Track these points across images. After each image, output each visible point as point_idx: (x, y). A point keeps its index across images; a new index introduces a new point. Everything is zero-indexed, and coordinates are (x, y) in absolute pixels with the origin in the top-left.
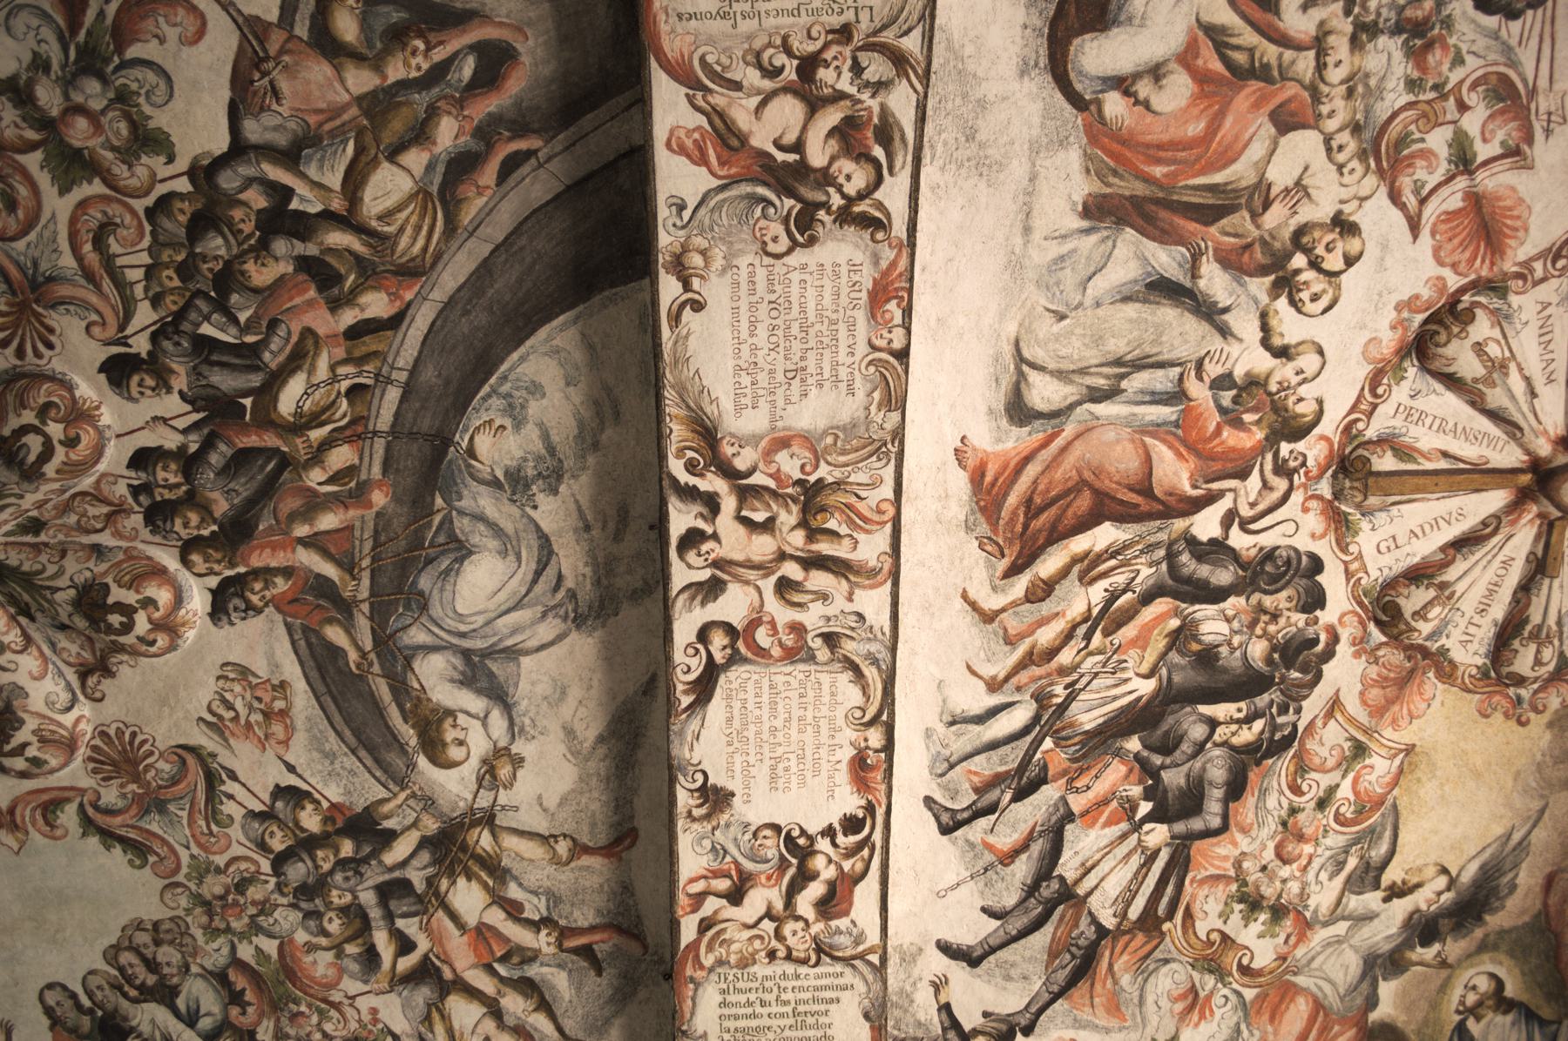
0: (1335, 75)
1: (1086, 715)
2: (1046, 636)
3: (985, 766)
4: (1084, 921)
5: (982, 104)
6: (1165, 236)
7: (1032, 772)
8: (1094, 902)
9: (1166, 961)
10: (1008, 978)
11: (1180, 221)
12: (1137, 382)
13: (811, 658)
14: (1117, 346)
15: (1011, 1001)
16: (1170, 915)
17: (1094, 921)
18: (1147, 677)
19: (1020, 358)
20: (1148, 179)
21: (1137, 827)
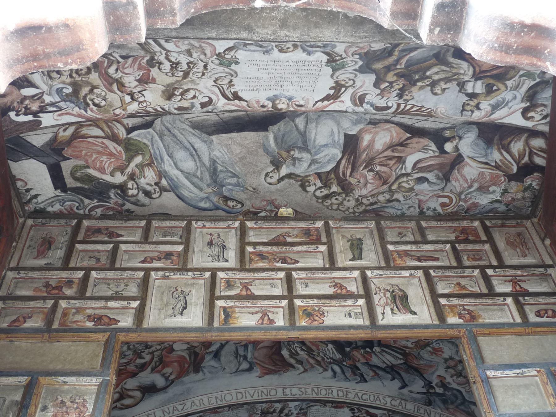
0: (159, 347)
1: (338, 356)
2: (312, 361)
3: (349, 373)
4: (400, 366)
5: (174, 395)
6: (203, 359)
7: (353, 367)
8: (394, 363)
9: (419, 354)
10: (413, 381)
11: (199, 358)
12: (241, 352)
13: (306, 412)
14: (232, 358)
15: (422, 383)
16: (405, 351)
17: (401, 364)
18: (327, 346)
19: (236, 372)
20: (189, 367)
21: (374, 352)
